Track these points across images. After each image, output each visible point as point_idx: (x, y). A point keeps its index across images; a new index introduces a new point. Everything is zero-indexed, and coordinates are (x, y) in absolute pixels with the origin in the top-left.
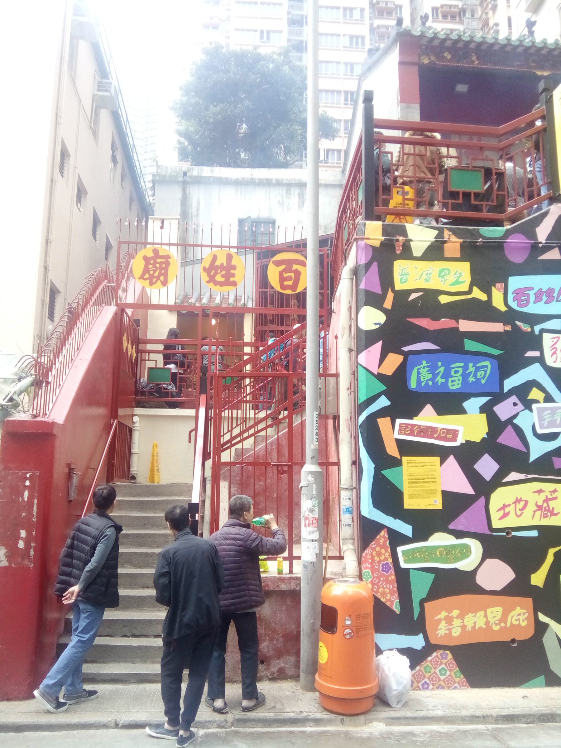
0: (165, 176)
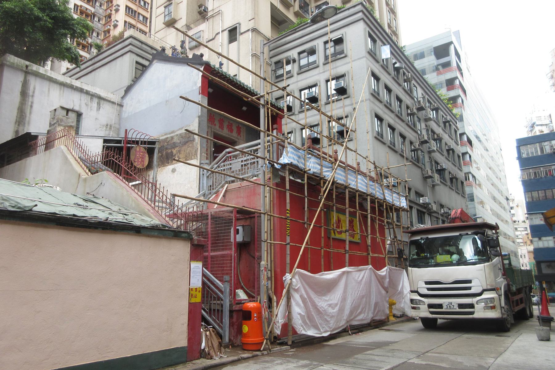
0: (13, 63)
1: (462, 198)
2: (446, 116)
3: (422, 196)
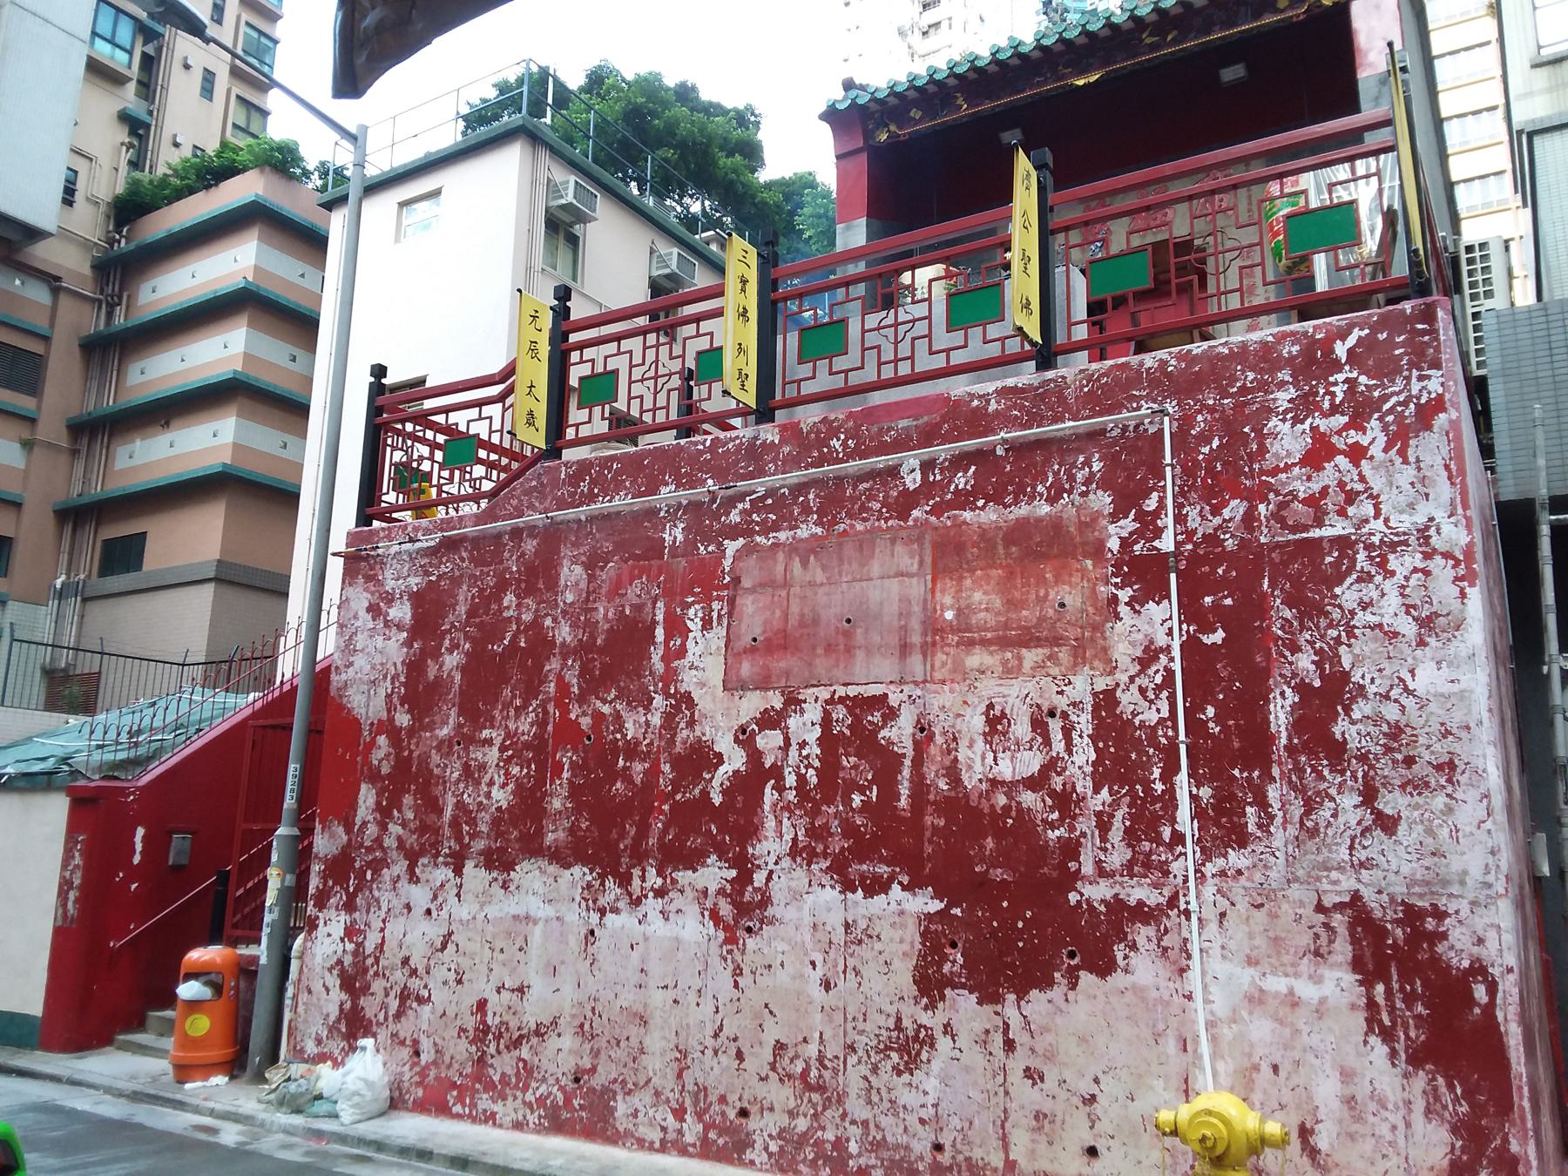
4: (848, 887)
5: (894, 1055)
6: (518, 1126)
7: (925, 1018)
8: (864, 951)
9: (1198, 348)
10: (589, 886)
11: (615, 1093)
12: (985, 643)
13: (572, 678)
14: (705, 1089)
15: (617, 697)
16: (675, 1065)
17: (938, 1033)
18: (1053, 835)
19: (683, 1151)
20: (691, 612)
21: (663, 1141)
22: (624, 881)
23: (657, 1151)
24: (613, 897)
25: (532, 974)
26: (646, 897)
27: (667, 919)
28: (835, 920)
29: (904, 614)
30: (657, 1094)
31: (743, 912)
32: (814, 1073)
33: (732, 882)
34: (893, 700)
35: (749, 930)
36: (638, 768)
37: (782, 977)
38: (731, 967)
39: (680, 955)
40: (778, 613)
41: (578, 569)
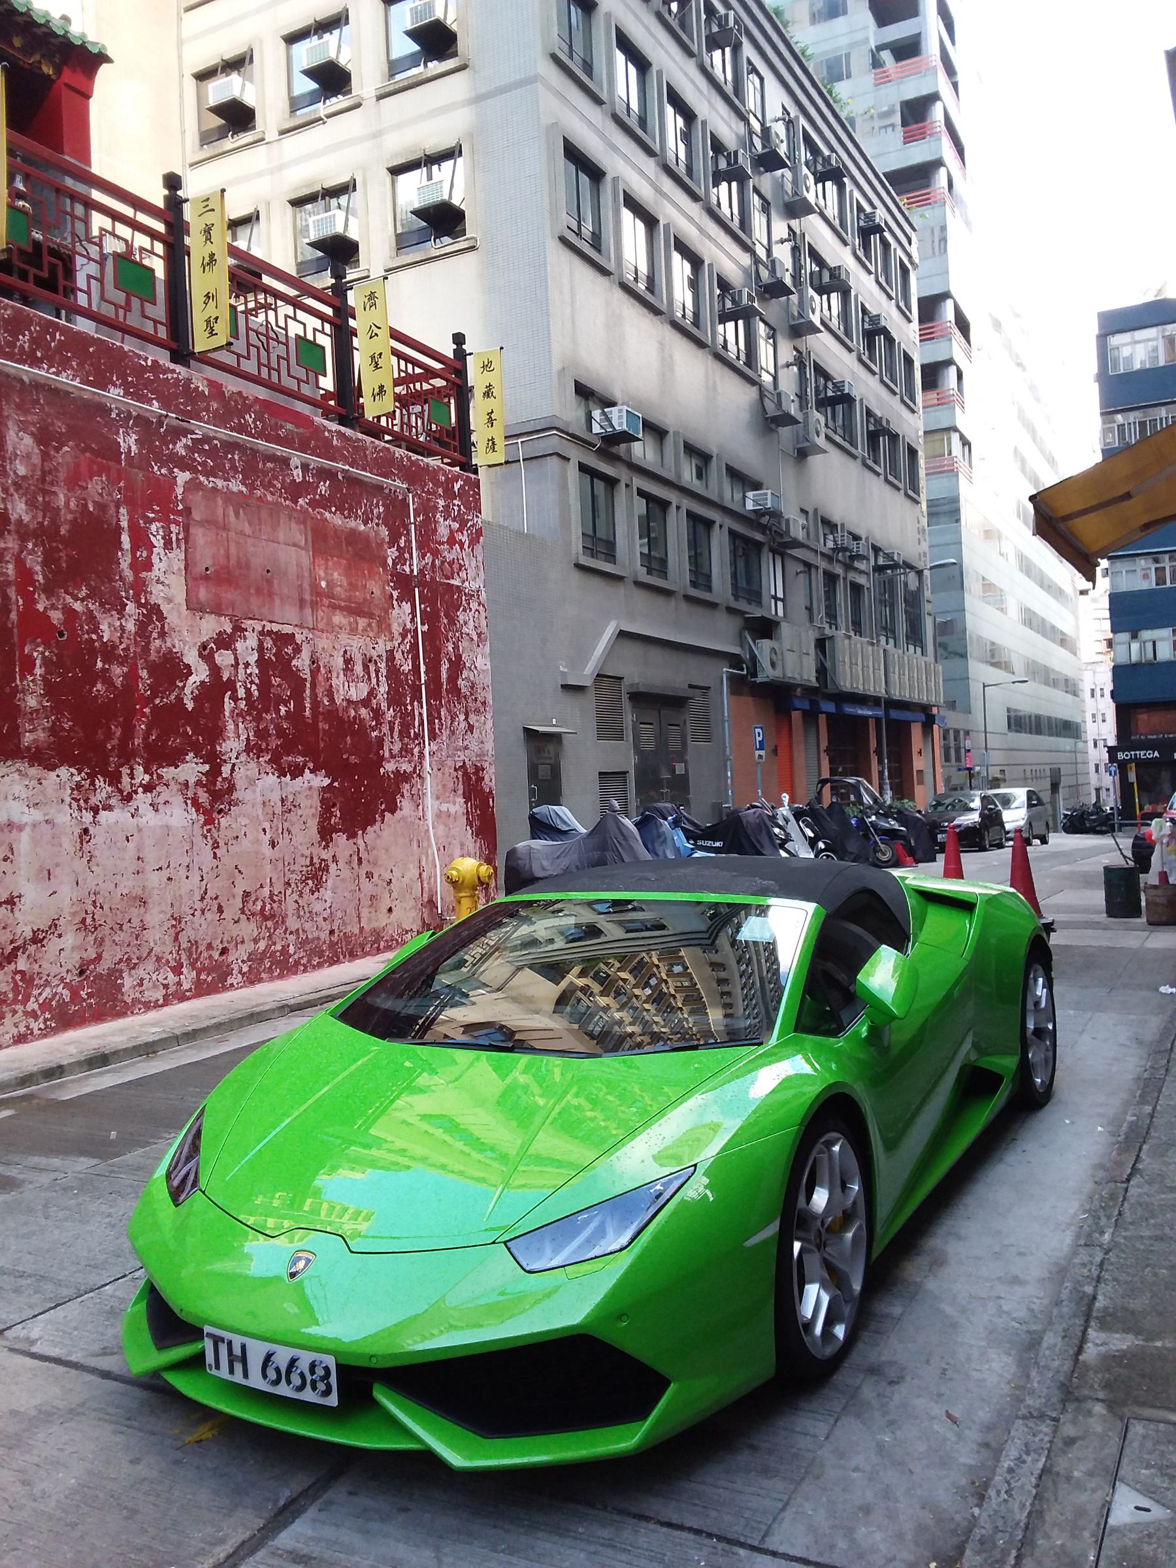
1: (908, 502)
2: (874, 207)
3: (757, 486)
4: (282, 774)
5: (310, 882)
6: (20, 1039)
7: (325, 855)
8: (292, 817)
9: (414, 457)
10: (79, 786)
11: (121, 971)
12: (341, 609)
13: (35, 562)
14: (196, 942)
15: (88, 596)
16: (172, 932)
17: (330, 863)
18: (374, 734)
19: (183, 998)
20: (153, 528)
21: (166, 997)
22: (114, 779)
23: (162, 1006)
24: (104, 795)
25: (23, 882)
26: (136, 792)
27: (157, 811)
28: (275, 798)
29: (300, 577)
30: (158, 959)
31: (215, 798)
32: (268, 907)
33: (206, 774)
34: (299, 638)
35: (220, 811)
36: (118, 672)
37: (245, 843)
38: (211, 842)
39: (170, 839)
40: (222, 552)
41: (28, 440)
